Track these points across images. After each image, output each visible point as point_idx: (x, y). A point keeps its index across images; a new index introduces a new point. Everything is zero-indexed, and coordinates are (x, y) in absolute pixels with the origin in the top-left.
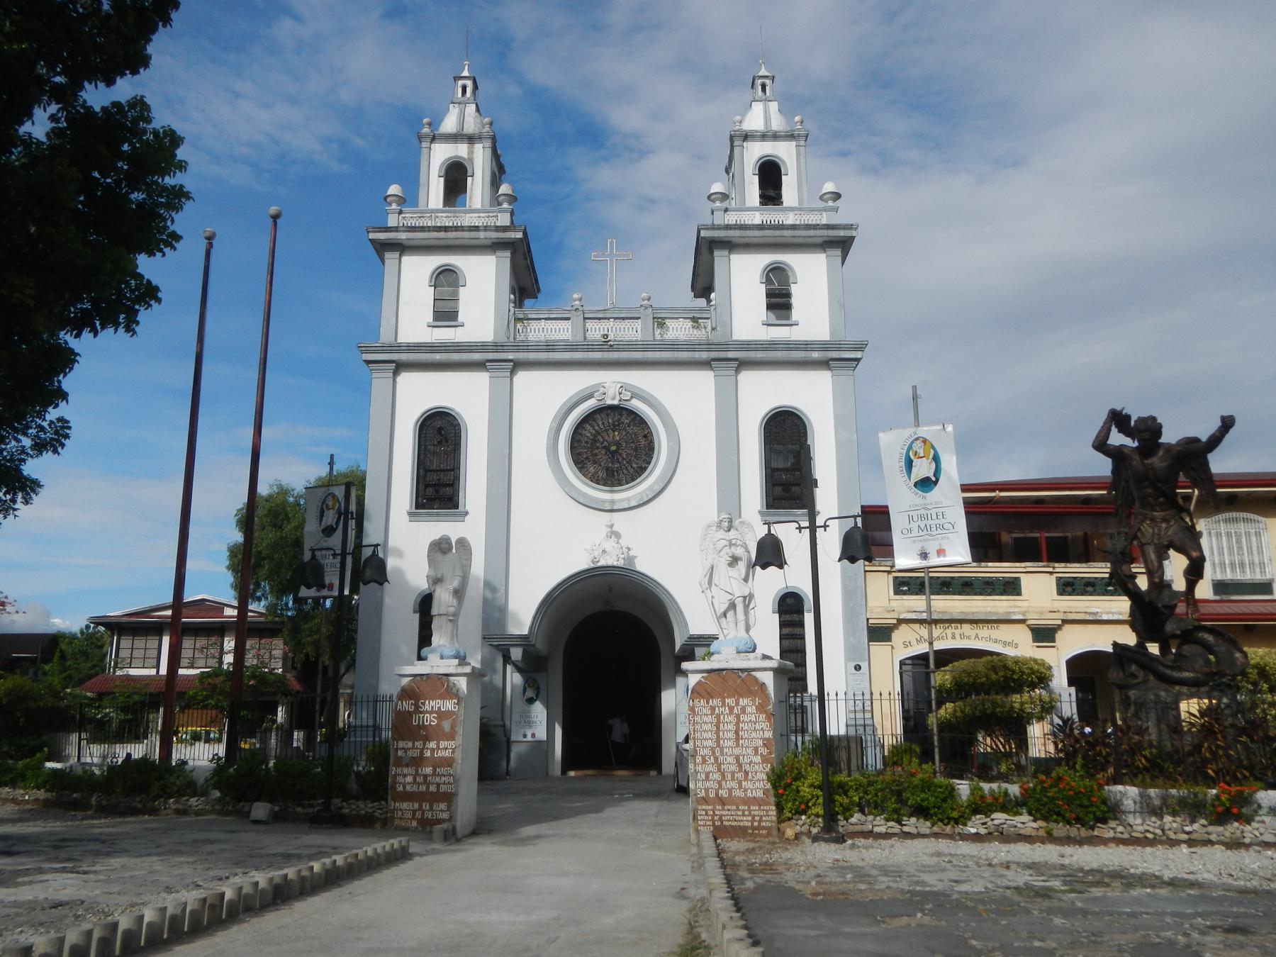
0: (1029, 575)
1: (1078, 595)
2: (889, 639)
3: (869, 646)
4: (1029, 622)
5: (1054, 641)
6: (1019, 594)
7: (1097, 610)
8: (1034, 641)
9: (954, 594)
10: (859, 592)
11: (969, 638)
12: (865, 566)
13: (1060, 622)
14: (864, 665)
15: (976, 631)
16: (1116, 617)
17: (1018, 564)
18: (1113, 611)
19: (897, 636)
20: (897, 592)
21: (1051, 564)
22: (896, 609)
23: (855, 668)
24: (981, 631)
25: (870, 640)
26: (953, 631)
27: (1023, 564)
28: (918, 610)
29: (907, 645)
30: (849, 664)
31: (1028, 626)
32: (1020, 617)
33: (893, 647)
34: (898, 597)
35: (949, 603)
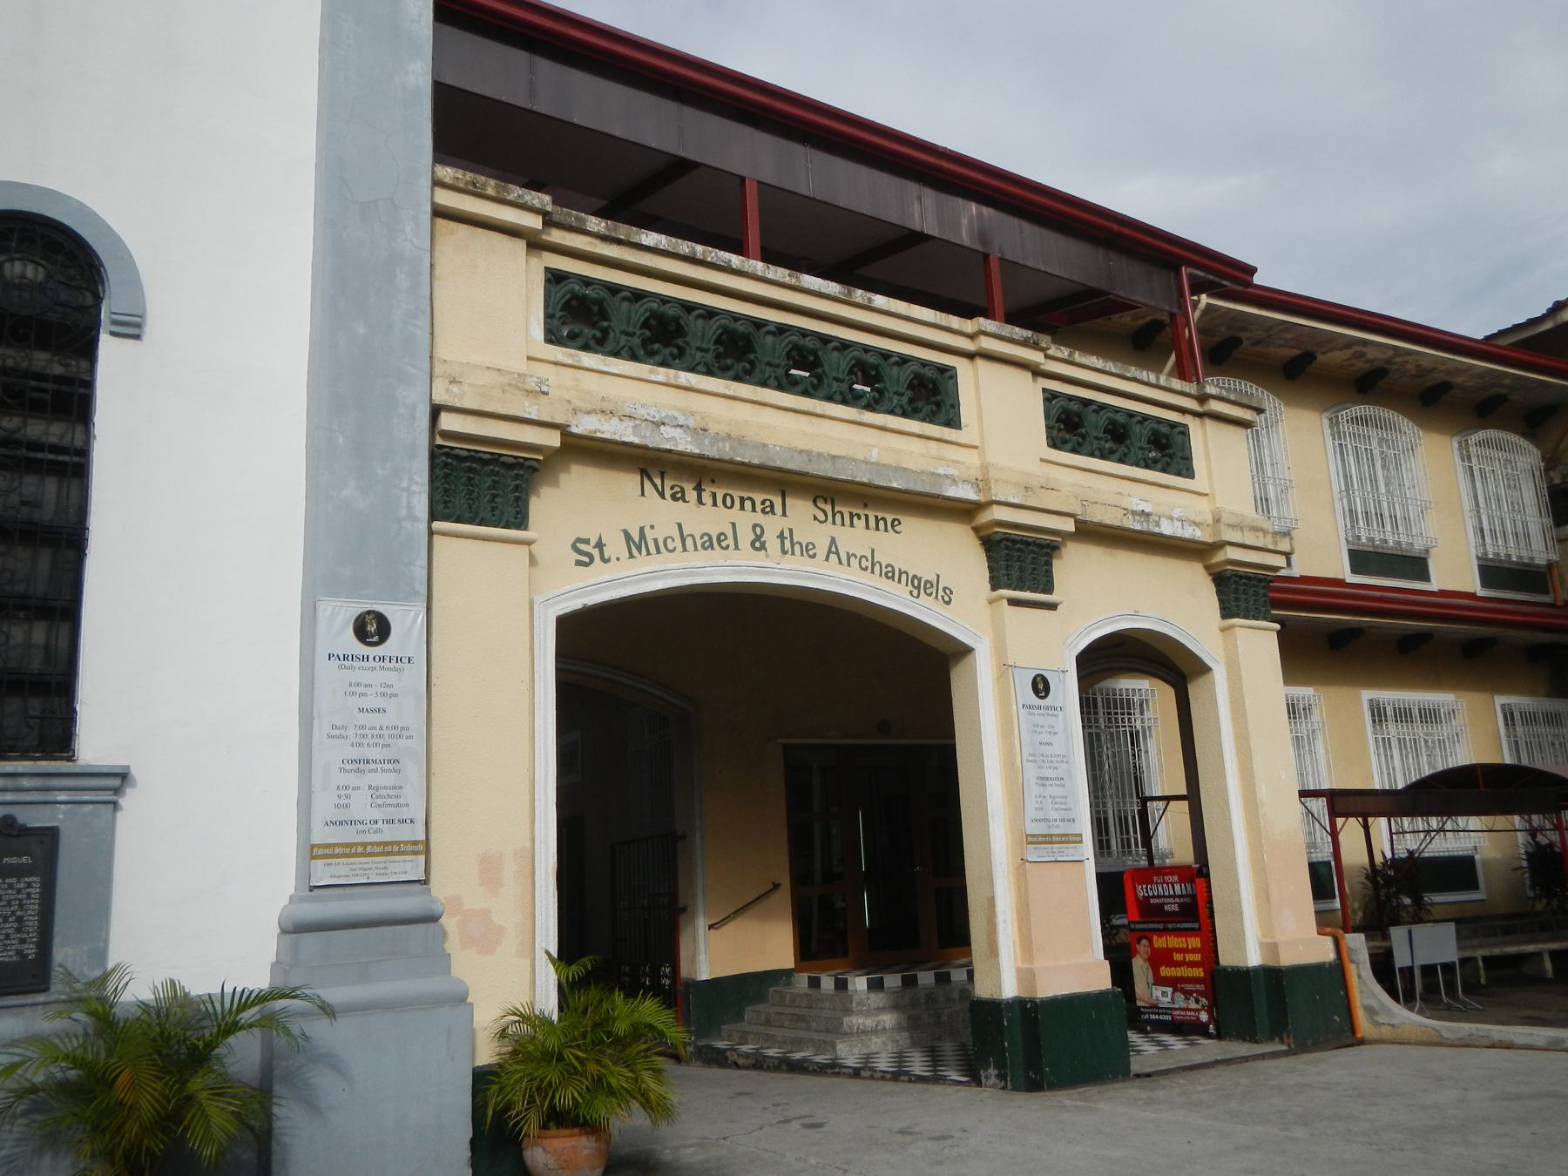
0: (980, 362)
1: (1092, 455)
2: (519, 519)
3: (431, 533)
4: (984, 518)
5: (1048, 589)
6: (953, 422)
7: (1147, 510)
8: (994, 588)
9: (763, 384)
10: (403, 281)
11: (808, 550)
12: (437, 183)
13: (1069, 526)
14: (405, 619)
15: (829, 530)
16: (1188, 532)
17: (954, 322)
18: (1176, 513)
19: (545, 505)
20: (552, 337)
21: (1045, 340)
22: (551, 392)
23: (361, 632)
24: (847, 528)
25: (433, 517)
26: (759, 518)
27: (969, 326)
28: (642, 412)
29: (587, 553)
30: (326, 608)
31: (976, 530)
32: (968, 493)
33: (533, 561)
34: (559, 353)
35: (743, 412)
